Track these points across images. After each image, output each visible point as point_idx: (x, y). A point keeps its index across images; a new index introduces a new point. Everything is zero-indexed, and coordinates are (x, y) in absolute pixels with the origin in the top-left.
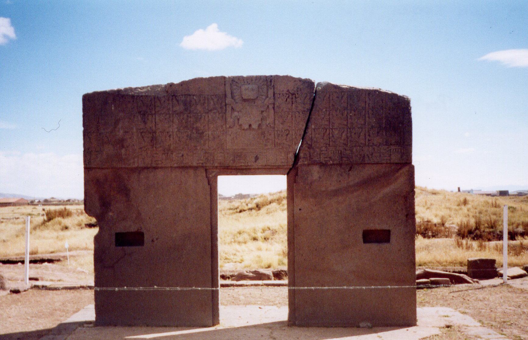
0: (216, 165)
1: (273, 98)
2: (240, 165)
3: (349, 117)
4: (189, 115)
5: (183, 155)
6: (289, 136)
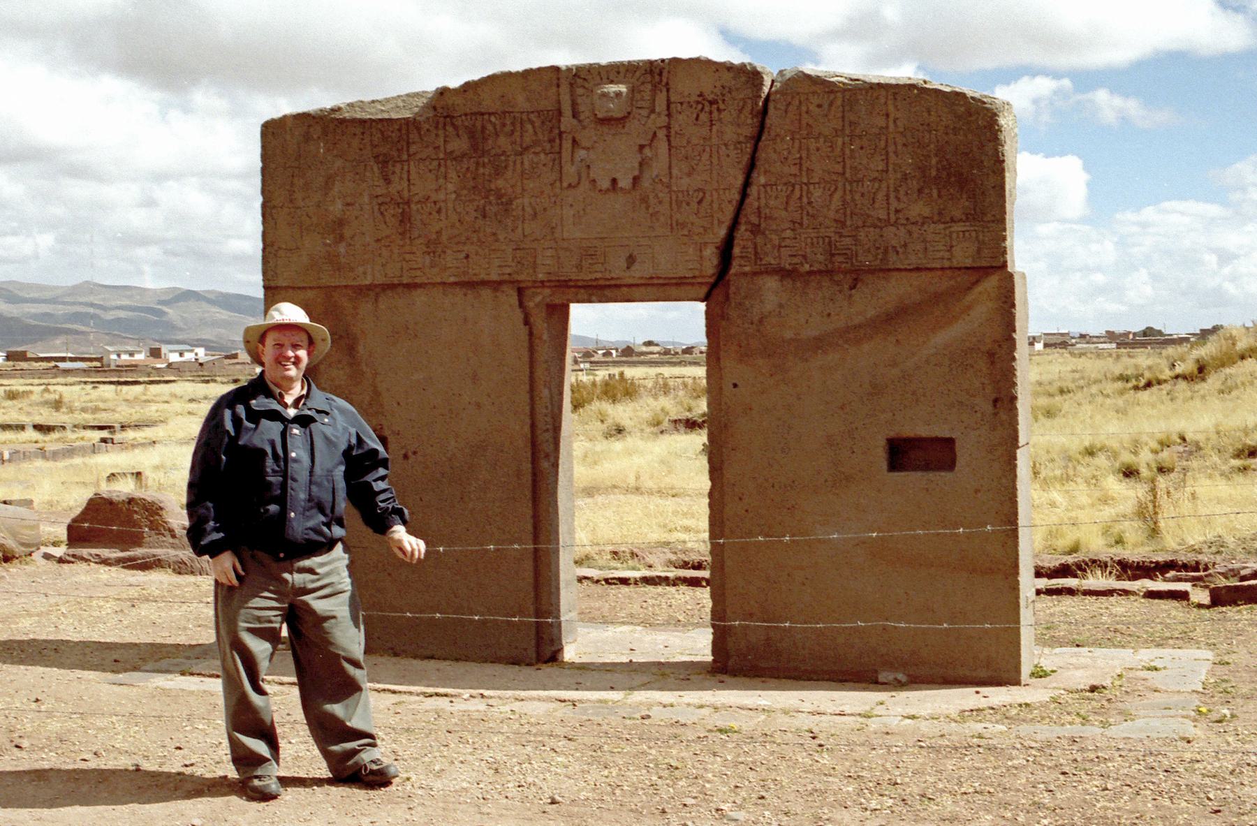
0: (541, 276)
1: (666, 113)
2: (594, 276)
3: (847, 152)
4: (481, 160)
5: (467, 257)
6: (704, 204)
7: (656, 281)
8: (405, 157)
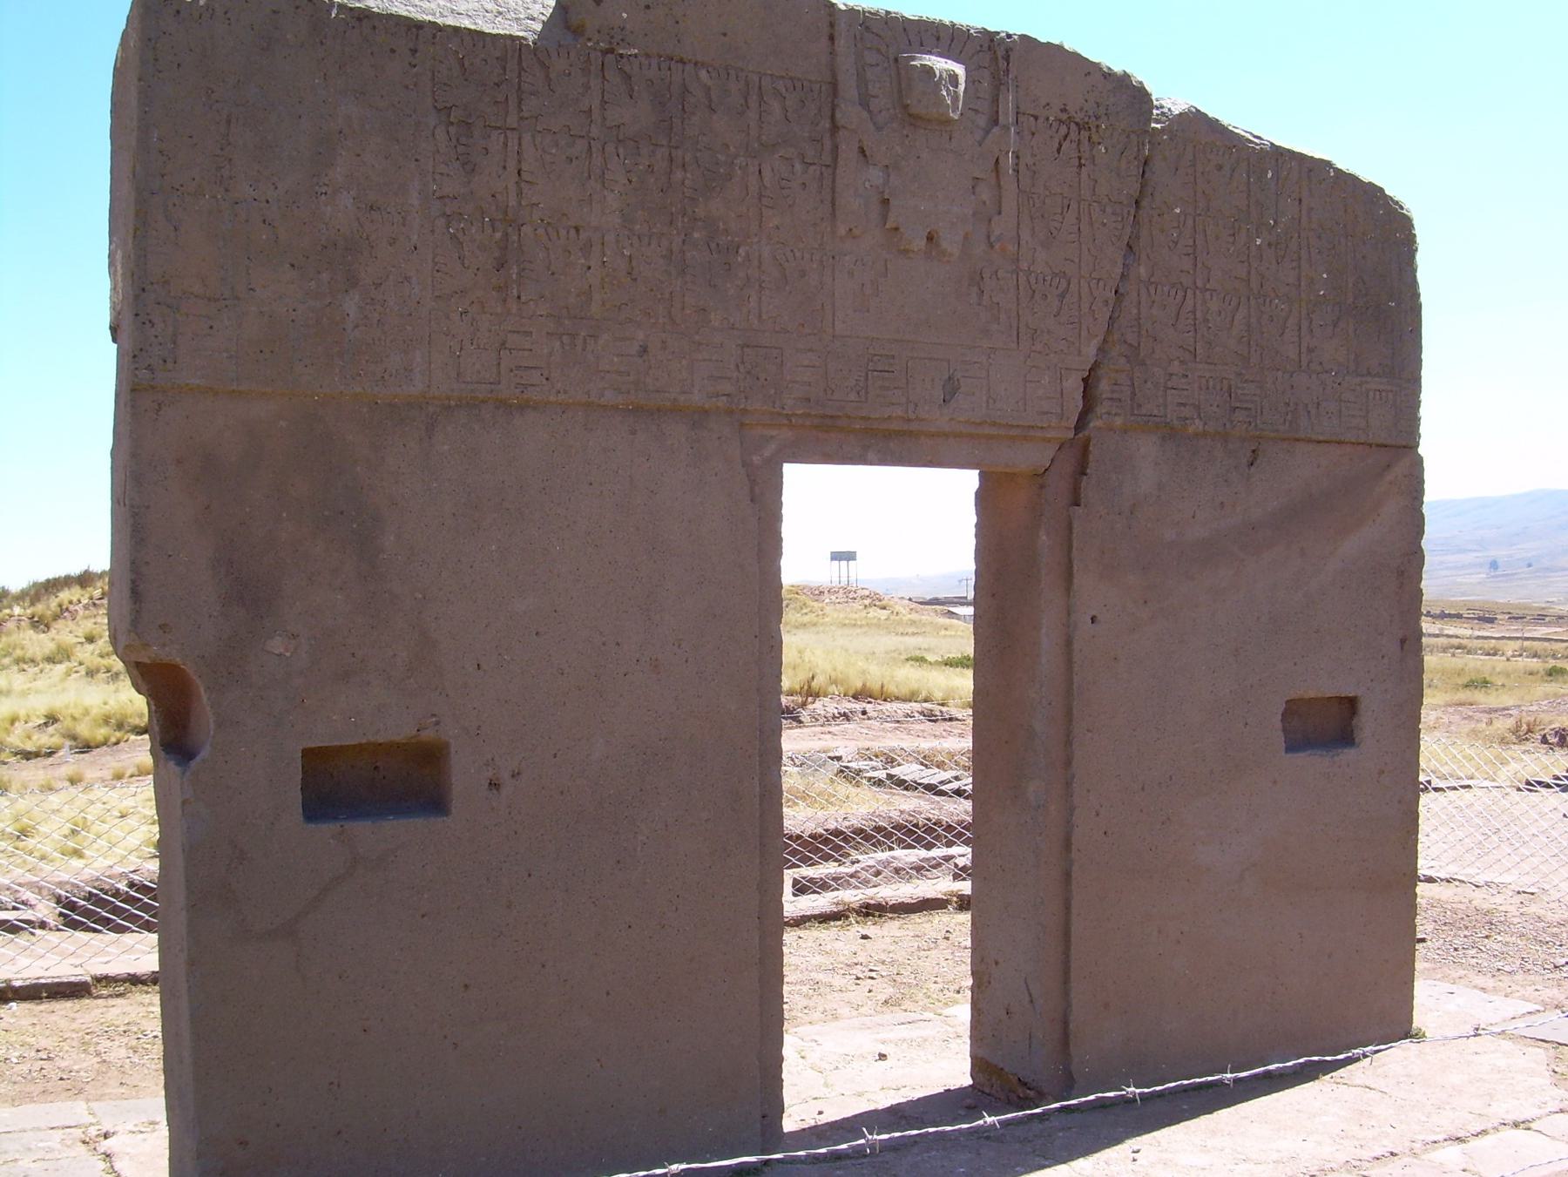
5: (644, 350)
7: (987, 431)
8: (512, 120)
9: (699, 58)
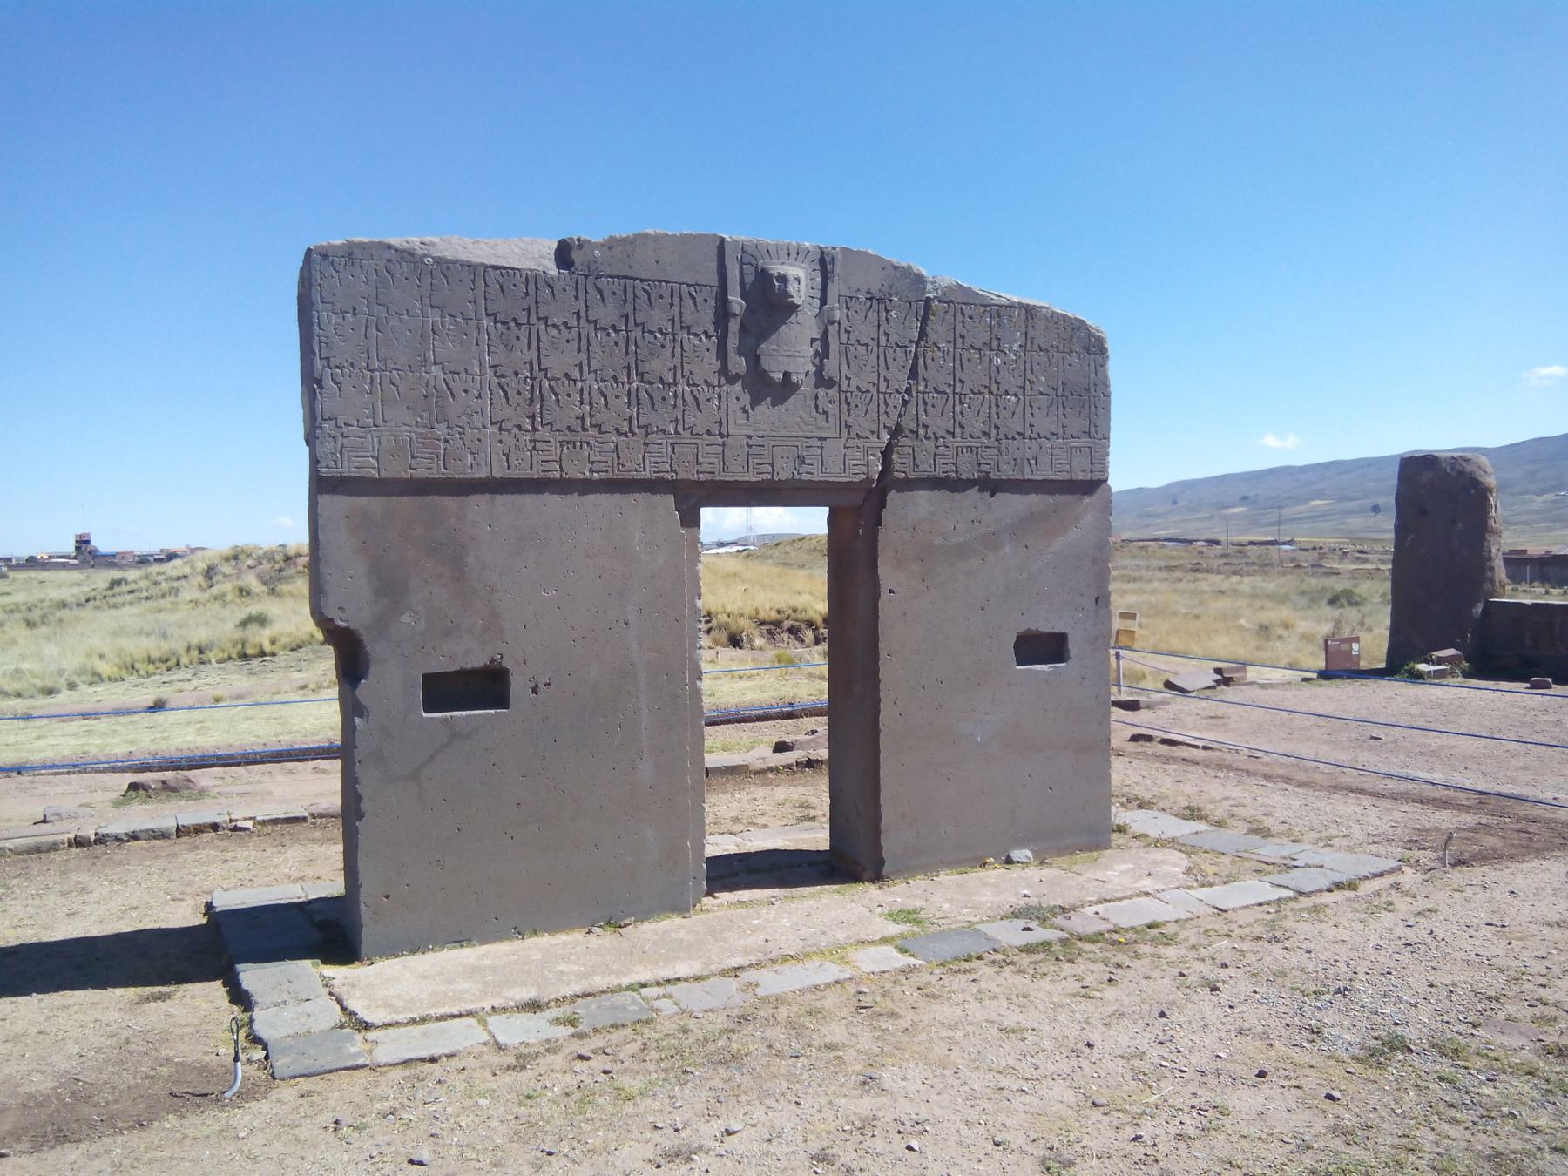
8: (533, 319)
9: (643, 277)
